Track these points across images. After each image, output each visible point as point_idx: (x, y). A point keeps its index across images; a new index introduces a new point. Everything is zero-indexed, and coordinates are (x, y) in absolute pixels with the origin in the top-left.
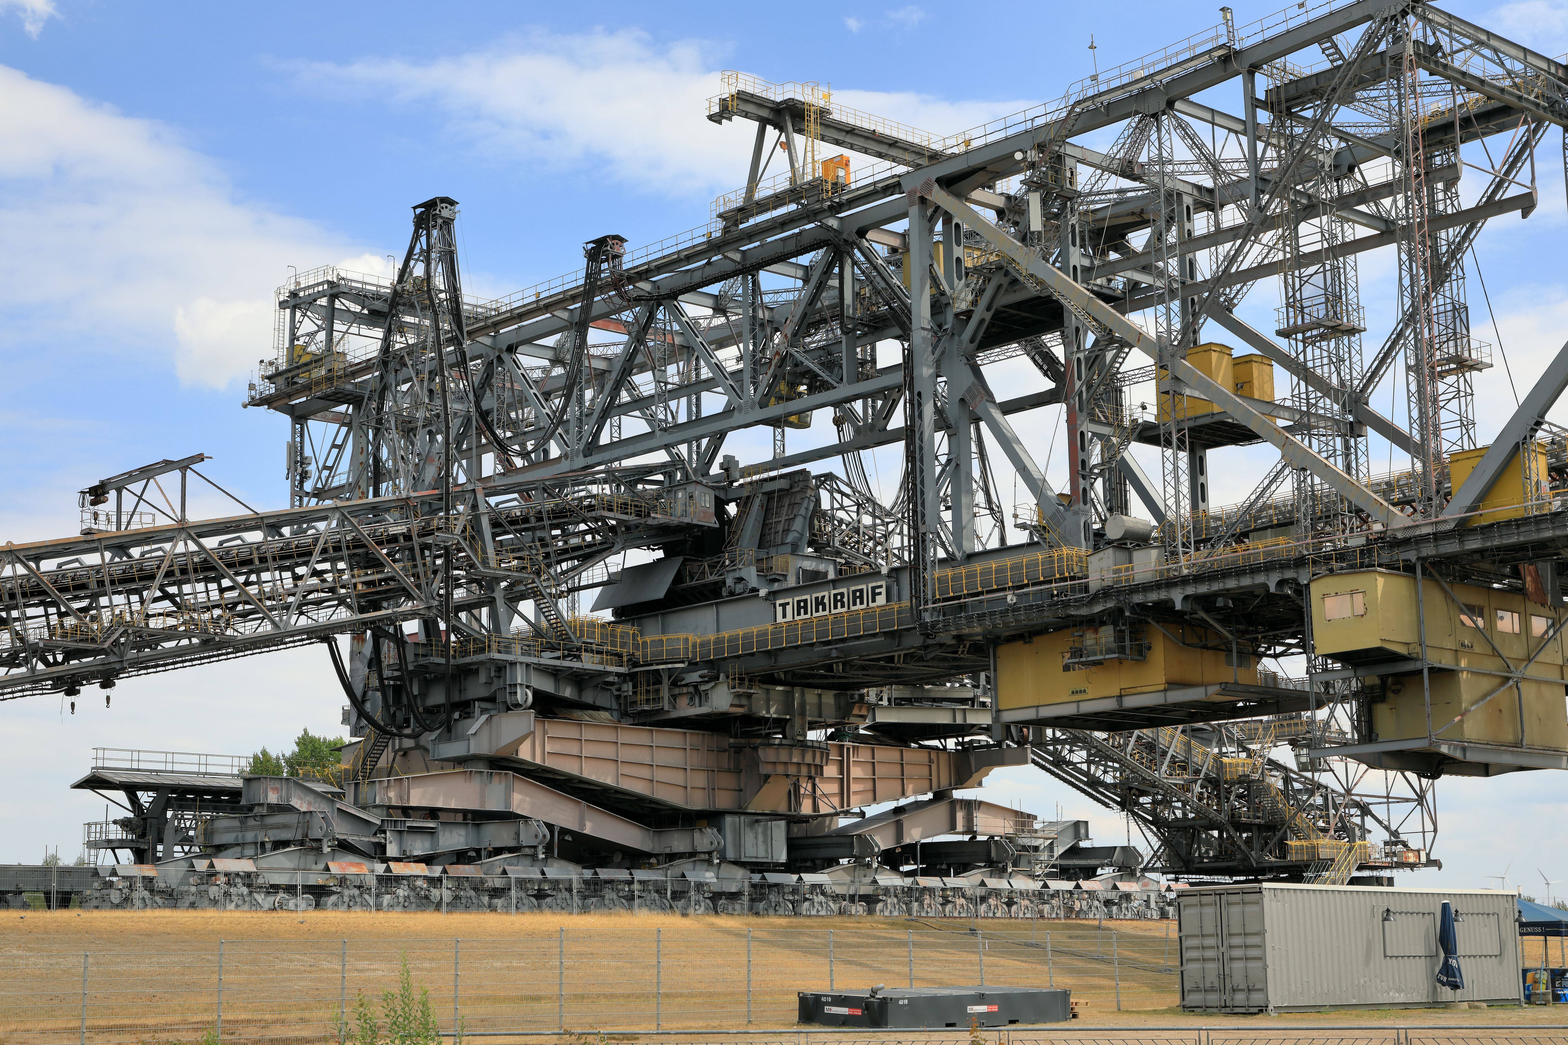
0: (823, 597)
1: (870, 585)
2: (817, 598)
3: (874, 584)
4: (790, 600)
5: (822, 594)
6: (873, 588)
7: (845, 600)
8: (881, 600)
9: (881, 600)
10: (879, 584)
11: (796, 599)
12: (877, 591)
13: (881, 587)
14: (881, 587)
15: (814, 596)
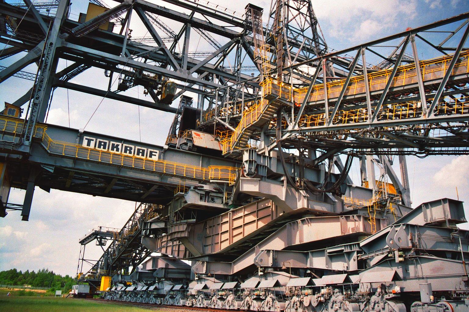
0: (118, 145)
1: (149, 150)
2: (113, 145)
3: (152, 150)
4: (94, 139)
5: (118, 143)
6: (151, 152)
7: (133, 151)
8: (155, 158)
9: (155, 158)
10: (155, 151)
11: (98, 140)
12: (153, 153)
13: (156, 153)
14: (156, 153)
15: (112, 142)
